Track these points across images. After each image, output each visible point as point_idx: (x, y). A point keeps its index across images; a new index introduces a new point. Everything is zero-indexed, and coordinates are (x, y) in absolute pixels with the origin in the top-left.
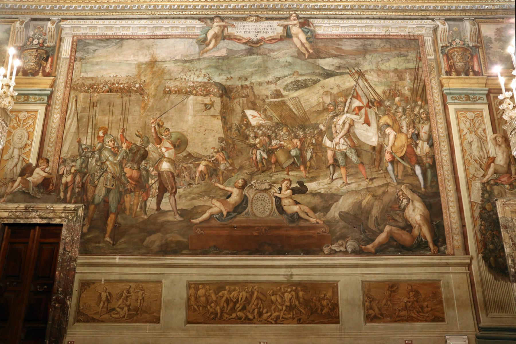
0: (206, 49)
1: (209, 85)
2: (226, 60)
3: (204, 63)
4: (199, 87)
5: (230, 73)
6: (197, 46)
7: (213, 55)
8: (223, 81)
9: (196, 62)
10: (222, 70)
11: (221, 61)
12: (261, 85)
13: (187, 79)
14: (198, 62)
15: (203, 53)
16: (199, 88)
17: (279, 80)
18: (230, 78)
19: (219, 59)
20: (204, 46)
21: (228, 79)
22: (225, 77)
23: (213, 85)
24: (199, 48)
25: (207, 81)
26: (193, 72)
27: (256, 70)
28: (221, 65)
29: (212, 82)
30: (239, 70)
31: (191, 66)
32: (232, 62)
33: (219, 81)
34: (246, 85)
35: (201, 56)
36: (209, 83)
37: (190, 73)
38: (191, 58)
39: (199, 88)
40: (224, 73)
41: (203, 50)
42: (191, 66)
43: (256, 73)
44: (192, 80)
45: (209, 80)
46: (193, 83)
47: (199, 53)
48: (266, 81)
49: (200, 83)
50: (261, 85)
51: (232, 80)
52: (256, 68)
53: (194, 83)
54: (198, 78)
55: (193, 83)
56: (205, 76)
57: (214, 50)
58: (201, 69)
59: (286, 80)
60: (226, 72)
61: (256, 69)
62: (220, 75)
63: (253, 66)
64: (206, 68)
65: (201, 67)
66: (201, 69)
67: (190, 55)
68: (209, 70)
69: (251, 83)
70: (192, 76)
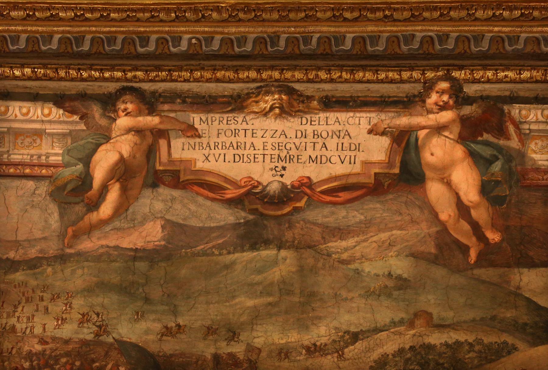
0: (86, 218)
1: (101, 351)
2: (163, 264)
3: (80, 272)
4: (62, 356)
5: (175, 312)
6: (53, 208)
7: (112, 243)
8: (151, 337)
9: (49, 270)
10: (147, 300)
11: (142, 266)
12: (287, 356)
13: (18, 326)
14: (58, 267)
15: (76, 236)
16: (64, 360)
17: (353, 343)
18: (174, 329)
19: (135, 259)
20: (79, 209)
21: (167, 332)
22: (157, 326)
23: (114, 354)
24: (61, 216)
25: (90, 337)
26: (42, 305)
27: (270, 304)
28: (142, 281)
29: (110, 340)
30: (208, 303)
31: (33, 283)
32: (184, 272)
33: (134, 339)
34: (231, 355)
35: (70, 247)
36: (101, 344)
37: (29, 310)
38: (33, 253)
39: (64, 360)
40: (153, 312)
41: (74, 224)
42: (33, 283)
43: (270, 315)
44: (38, 330)
45: (97, 335)
46: (42, 341)
47: (62, 235)
48: (306, 343)
49: (67, 342)
50: (287, 356)
51: (183, 336)
52: (270, 294)
53: (46, 343)
54: (58, 327)
55: (42, 341)
56: (84, 319)
57: (117, 224)
58: (70, 295)
59: (380, 344)
60: (161, 308)
61: (270, 299)
62: (139, 316)
63: (260, 288)
64: (89, 291)
65: (70, 286)
66: (70, 295)
67: (28, 241)
68: (100, 300)
69: (250, 348)
70: (38, 320)
